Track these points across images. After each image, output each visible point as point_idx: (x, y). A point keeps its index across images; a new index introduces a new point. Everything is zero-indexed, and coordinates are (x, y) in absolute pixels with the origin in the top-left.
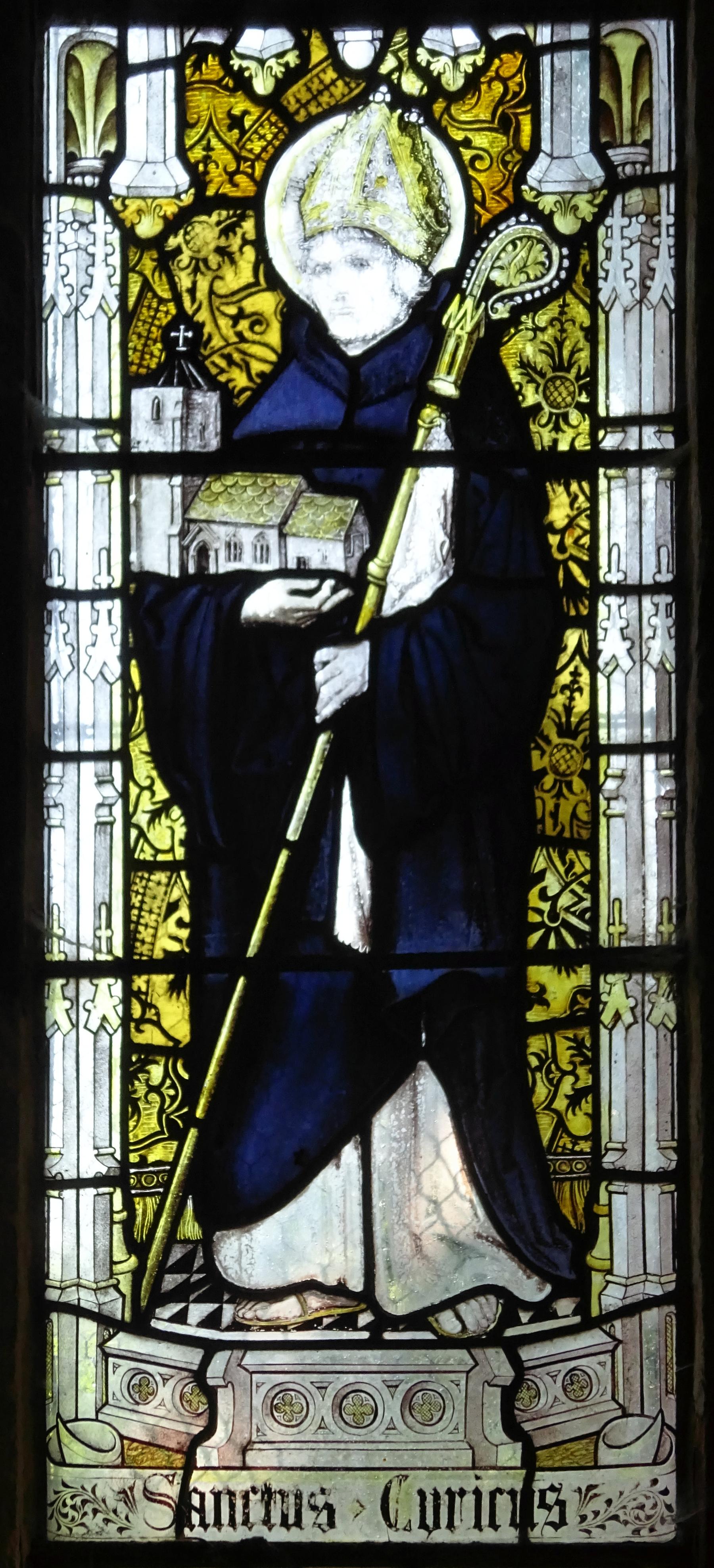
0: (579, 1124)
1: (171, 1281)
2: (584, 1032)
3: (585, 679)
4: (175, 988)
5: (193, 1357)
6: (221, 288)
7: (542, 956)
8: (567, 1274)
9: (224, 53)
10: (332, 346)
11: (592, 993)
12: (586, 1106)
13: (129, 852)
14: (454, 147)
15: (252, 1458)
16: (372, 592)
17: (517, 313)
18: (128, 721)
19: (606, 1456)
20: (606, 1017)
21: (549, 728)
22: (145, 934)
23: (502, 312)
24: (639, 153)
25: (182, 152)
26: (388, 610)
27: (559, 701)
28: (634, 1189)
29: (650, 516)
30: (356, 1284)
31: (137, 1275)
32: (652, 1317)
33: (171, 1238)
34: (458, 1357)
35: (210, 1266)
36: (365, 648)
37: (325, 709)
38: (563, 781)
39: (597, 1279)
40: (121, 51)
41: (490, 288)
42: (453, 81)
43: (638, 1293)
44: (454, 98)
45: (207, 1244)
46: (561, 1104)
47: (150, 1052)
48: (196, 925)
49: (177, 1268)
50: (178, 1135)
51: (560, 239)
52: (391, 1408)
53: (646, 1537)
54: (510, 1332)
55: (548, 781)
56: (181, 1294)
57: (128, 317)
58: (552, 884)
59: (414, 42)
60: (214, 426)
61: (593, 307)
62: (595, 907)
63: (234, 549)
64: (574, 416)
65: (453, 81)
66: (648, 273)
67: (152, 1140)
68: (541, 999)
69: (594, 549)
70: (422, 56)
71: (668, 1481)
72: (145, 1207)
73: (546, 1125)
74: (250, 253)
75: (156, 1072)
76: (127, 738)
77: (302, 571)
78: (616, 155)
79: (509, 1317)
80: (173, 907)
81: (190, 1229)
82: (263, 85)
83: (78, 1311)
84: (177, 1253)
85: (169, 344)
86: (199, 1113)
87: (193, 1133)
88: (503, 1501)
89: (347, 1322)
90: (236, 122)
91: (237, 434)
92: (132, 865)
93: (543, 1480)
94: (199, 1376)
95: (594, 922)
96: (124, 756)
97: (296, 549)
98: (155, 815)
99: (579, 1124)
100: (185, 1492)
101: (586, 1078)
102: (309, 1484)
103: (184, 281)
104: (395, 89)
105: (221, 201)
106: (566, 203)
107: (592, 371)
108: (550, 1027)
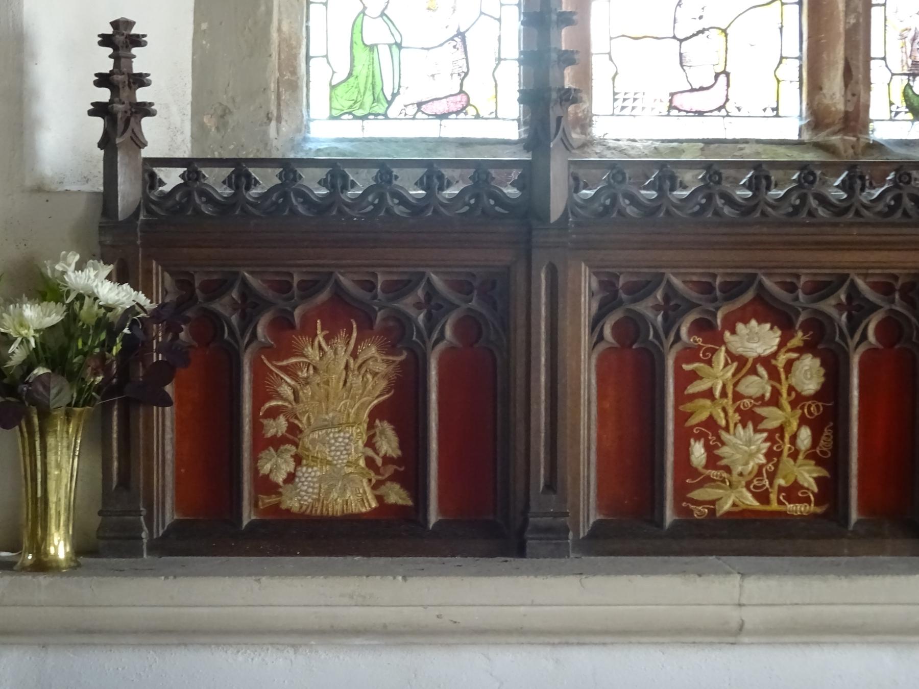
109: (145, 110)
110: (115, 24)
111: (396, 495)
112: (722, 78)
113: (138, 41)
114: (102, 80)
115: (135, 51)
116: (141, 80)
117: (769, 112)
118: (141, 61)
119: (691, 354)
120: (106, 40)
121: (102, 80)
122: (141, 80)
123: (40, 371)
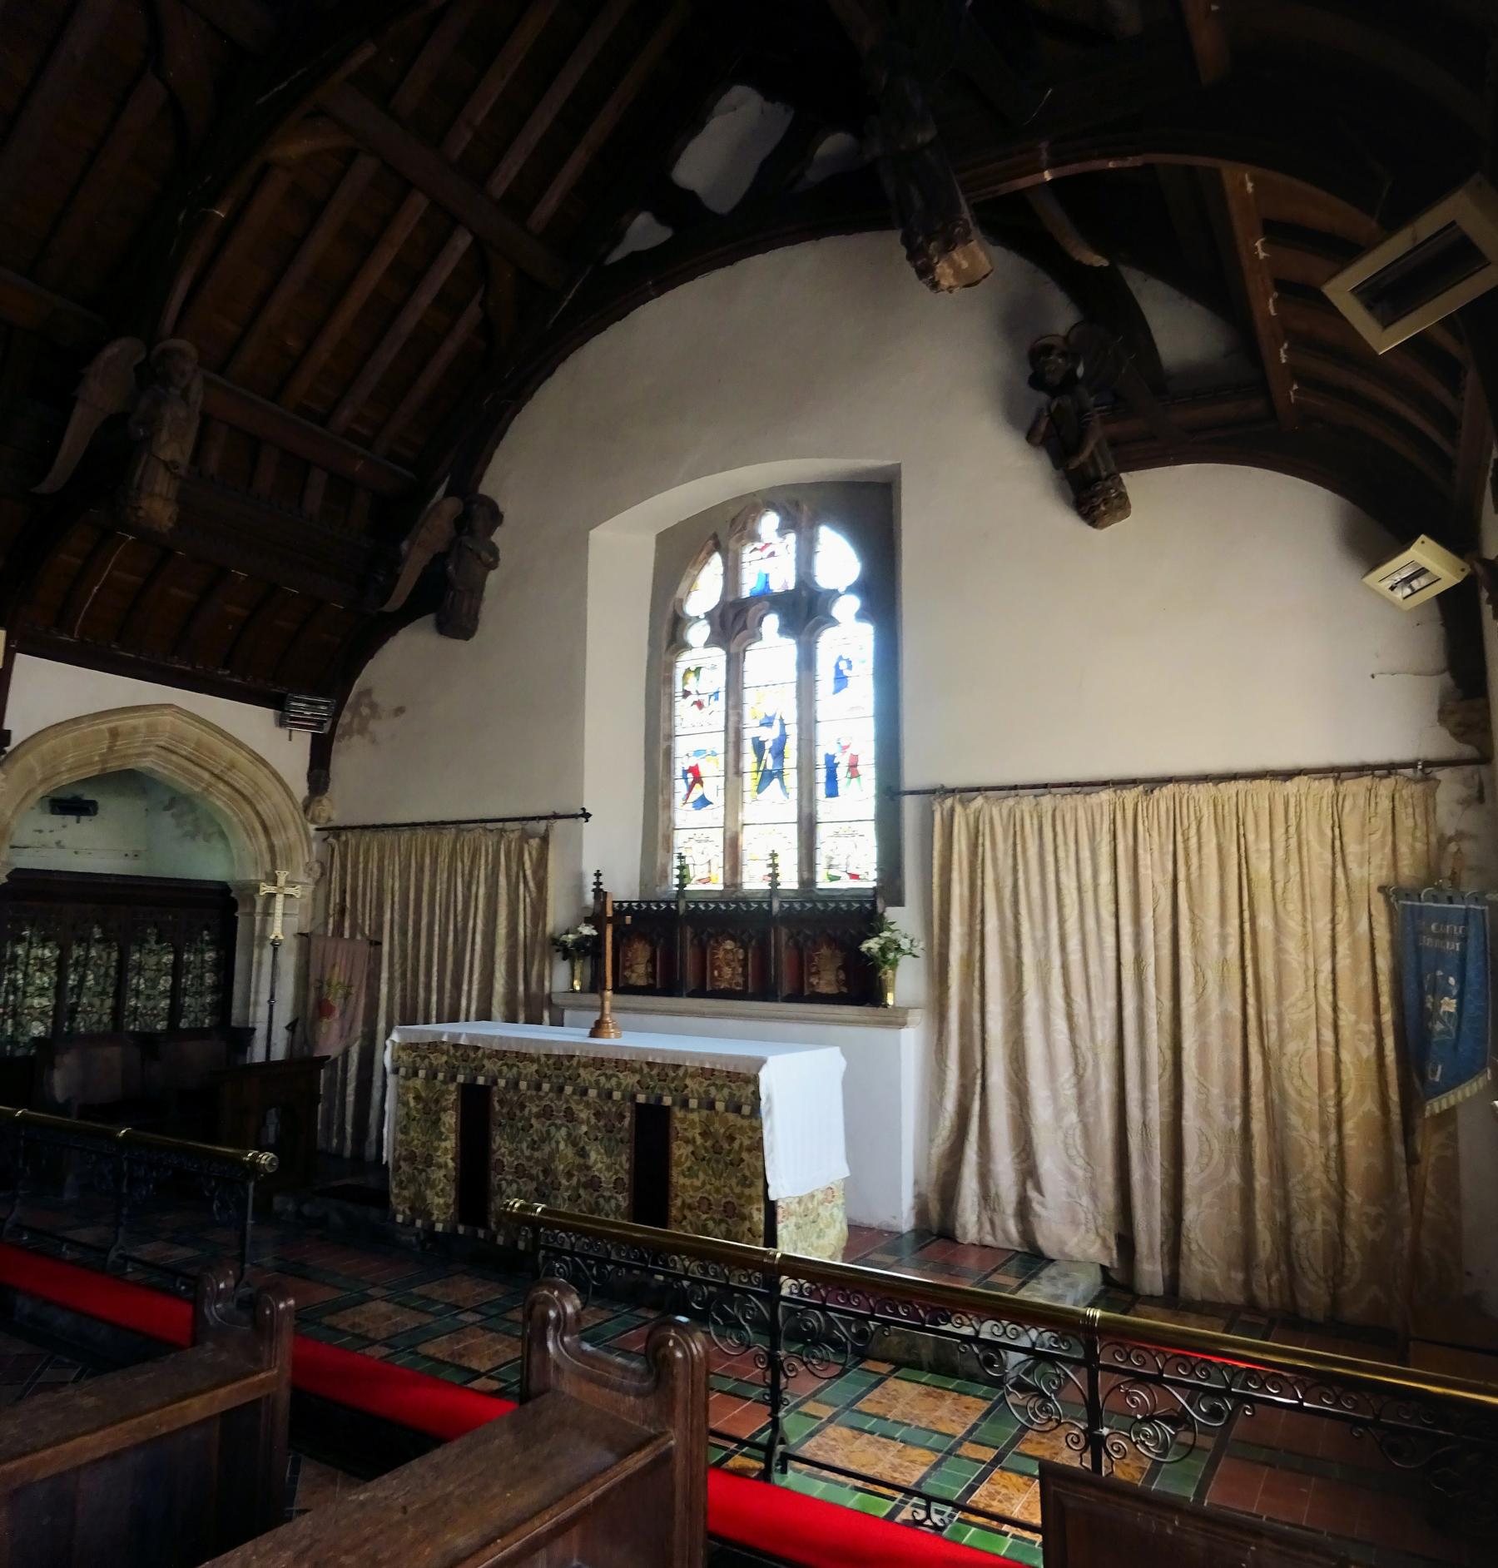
111: (651, 981)
113: (600, 875)
114: (595, 884)
116: (601, 884)
118: (601, 879)
119: (714, 948)
120: (595, 874)
122: (601, 884)
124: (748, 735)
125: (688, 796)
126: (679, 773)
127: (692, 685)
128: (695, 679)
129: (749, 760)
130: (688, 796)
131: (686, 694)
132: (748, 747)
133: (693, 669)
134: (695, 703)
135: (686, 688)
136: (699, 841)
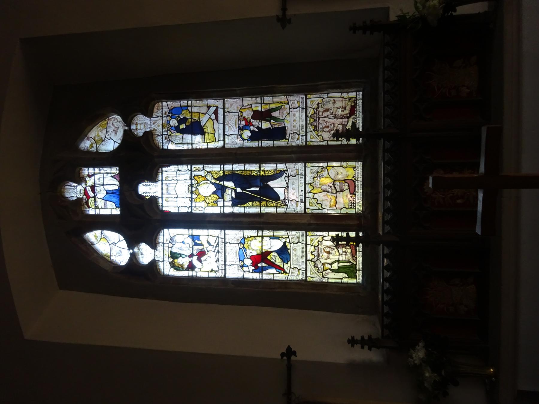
0: (272, 171)
1: (284, 203)
2: (265, 171)
3: (239, 171)
4: (262, 203)
5: (290, 201)
6: (211, 199)
7: (260, 174)
8: (284, 172)
9: (194, 199)
10: (215, 191)
11: (262, 170)
12: (271, 171)
13: (252, 206)
14: (201, 182)
15: (297, 197)
16: (233, 188)
17: (213, 177)
18: (242, 206)
19: (297, 169)
20: (264, 169)
21: (243, 174)
22: (258, 205)
23: (213, 178)
24: (202, 168)
25: (201, 202)
26: (234, 186)
27: (241, 173)
28: (277, 167)
29: (227, 167)
30: (284, 188)
31: (283, 206)
32: (287, 165)
33: (281, 203)
34: (290, 181)
35: (283, 200)
36: (237, 188)
37: (242, 191)
38: (247, 173)
39: (284, 170)
40: (194, 207)
41: (211, 179)
42: (196, 182)
43: (285, 167)
44: (198, 182)
45: (281, 200)
46: (271, 173)
47: (266, 204)
48: (257, 201)
49: (283, 203)
50: (273, 202)
51: (208, 173)
52: (294, 186)
53: (304, 165)
54: (288, 176)
55: (247, 174)
56: (285, 202)
57: (213, 206)
58: (254, 174)
59: (194, 185)
60: (221, 200)
61: (212, 171)
62: (256, 170)
63: (230, 198)
64: (220, 172)
65: (196, 182)
66: (210, 167)
67: (273, 204)
68: (263, 174)
69: (230, 171)
70: (195, 184)
71: (299, 164)
72: (278, 205)
73: (272, 174)
74: (208, 197)
75: (268, 204)
76: (243, 206)
77: (231, 193)
78: (202, 170)
79: (287, 177)
80: (256, 203)
81: (280, 201)
82: (197, 196)
83: (286, 210)
84: (282, 202)
85: (215, 203)
86: (271, 201)
87: (273, 201)
88: (301, 177)
89: (287, 189)
90: (199, 198)
91: (221, 198)
92: (253, 206)
93: (299, 174)
94: (291, 201)
95: (257, 170)
96: (245, 207)
97: (230, 193)
98: (249, 204)
99: (272, 171)
100: (300, 202)
101: (269, 171)
102: (299, 192)
103: (211, 202)
104: (197, 186)
105: (205, 199)
106: (205, 173)
107: (217, 171)
108: (265, 174)
109: (370, 337)
110: (349, 343)
112: (346, 181)
113: (353, 338)
115: (355, 339)
116: (362, 338)
117: (355, 169)
120: (353, 346)
121: (363, 347)
123: (443, 373)
124: (228, 210)
125: (277, 267)
126: (257, 276)
127: (184, 261)
128: (180, 259)
129: (251, 208)
130: (277, 267)
131: (191, 267)
132: (238, 210)
133: (171, 260)
134: (199, 260)
135: (186, 266)
136: (318, 255)
